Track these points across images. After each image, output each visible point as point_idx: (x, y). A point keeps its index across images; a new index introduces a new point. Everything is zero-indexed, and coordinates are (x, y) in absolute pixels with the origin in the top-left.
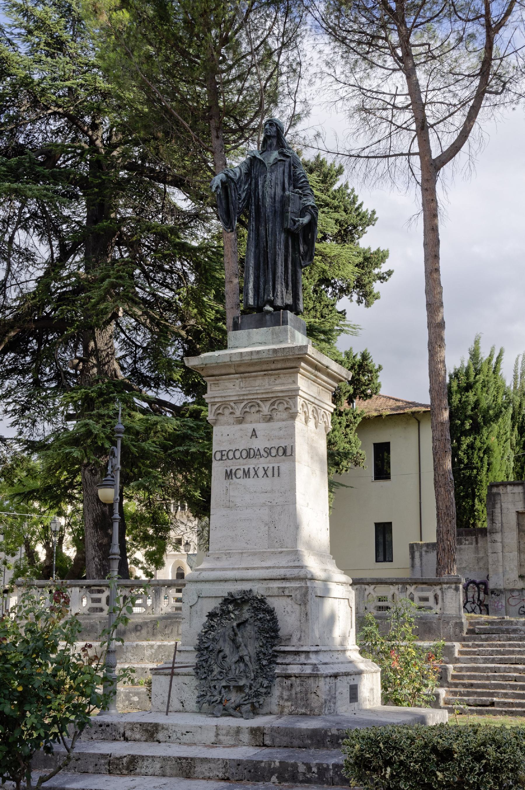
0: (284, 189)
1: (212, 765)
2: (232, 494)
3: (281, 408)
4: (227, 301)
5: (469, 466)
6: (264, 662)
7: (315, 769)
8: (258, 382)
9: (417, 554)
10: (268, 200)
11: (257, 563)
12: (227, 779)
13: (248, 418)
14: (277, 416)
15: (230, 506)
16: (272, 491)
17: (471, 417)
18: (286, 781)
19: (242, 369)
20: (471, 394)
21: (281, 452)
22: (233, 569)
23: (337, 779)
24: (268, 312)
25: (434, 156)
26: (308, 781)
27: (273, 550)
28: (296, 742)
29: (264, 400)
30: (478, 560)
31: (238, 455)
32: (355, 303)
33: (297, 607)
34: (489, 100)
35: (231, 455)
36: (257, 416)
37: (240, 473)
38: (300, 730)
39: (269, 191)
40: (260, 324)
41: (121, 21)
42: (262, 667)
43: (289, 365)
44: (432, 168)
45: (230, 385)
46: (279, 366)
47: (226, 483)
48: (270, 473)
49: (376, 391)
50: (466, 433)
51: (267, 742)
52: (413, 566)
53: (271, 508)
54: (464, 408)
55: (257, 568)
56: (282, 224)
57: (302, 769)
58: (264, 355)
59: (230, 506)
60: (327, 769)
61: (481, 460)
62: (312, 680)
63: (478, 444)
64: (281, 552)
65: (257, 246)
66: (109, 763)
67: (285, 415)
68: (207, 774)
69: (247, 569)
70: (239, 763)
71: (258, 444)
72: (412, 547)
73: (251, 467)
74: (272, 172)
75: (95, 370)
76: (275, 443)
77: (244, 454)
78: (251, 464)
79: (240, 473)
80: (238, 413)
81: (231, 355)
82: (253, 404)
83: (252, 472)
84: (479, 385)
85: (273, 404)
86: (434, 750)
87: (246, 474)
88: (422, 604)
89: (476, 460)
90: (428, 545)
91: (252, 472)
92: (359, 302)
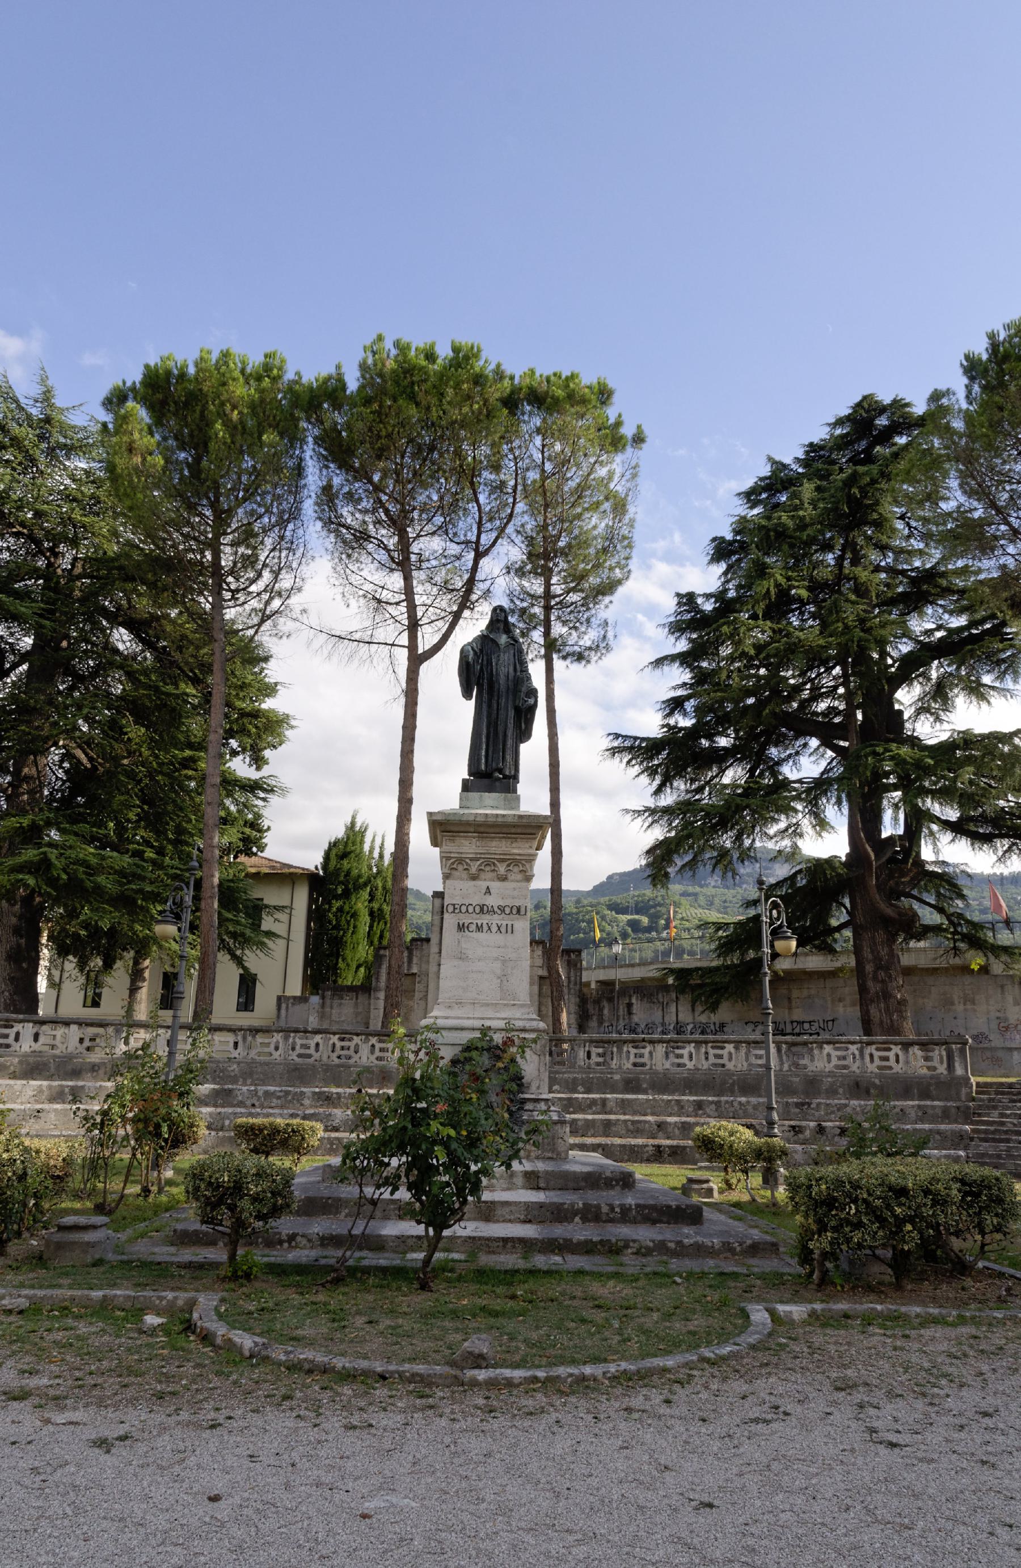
1: (513, 1208)
3: (516, 869)
4: (210, 750)
5: (337, 927)
7: (617, 1210)
8: (494, 843)
9: (284, 1006)
11: (490, 1014)
12: (530, 1221)
13: (483, 875)
14: (512, 876)
15: (462, 957)
16: (505, 947)
17: (342, 883)
18: (589, 1221)
19: (482, 829)
20: (345, 862)
23: (639, 1218)
25: (420, 651)
26: (611, 1221)
30: (357, 1014)
31: (471, 909)
32: (246, 766)
34: (466, 613)
37: (473, 927)
38: (575, 1172)
39: (503, 671)
40: (490, 790)
41: (155, 466)
42: (511, 1114)
44: (416, 660)
45: (466, 843)
46: (519, 831)
48: (503, 929)
49: (262, 848)
50: (337, 897)
51: (542, 1185)
52: (278, 1016)
53: (504, 962)
54: (338, 875)
56: (514, 701)
57: (605, 1209)
58: (510, 820)
59: (462, 957)
60: (630, 1209)
61: (348, 922)
62: (558, 1127)
63: (347, 908)
65: (489, 716)
66: (399, 1209)
67: (520, 877)
68: (508, 1217)
70: (541, 1205)
71: (492, 901)
75: (26, 797)
76: (509, 902)
77: (478, 909)
78: (484, 920)
79: (473, 927)
80: (474, 870)
82: (490, 863)
83: (485, 928)
84: (353, 855)
86: (891, 1188)
87: (479, 928)
88: (381, 1054)
89: (343, 922)
90: (295, 998)
91: (485, 928)
92: (250, 765)
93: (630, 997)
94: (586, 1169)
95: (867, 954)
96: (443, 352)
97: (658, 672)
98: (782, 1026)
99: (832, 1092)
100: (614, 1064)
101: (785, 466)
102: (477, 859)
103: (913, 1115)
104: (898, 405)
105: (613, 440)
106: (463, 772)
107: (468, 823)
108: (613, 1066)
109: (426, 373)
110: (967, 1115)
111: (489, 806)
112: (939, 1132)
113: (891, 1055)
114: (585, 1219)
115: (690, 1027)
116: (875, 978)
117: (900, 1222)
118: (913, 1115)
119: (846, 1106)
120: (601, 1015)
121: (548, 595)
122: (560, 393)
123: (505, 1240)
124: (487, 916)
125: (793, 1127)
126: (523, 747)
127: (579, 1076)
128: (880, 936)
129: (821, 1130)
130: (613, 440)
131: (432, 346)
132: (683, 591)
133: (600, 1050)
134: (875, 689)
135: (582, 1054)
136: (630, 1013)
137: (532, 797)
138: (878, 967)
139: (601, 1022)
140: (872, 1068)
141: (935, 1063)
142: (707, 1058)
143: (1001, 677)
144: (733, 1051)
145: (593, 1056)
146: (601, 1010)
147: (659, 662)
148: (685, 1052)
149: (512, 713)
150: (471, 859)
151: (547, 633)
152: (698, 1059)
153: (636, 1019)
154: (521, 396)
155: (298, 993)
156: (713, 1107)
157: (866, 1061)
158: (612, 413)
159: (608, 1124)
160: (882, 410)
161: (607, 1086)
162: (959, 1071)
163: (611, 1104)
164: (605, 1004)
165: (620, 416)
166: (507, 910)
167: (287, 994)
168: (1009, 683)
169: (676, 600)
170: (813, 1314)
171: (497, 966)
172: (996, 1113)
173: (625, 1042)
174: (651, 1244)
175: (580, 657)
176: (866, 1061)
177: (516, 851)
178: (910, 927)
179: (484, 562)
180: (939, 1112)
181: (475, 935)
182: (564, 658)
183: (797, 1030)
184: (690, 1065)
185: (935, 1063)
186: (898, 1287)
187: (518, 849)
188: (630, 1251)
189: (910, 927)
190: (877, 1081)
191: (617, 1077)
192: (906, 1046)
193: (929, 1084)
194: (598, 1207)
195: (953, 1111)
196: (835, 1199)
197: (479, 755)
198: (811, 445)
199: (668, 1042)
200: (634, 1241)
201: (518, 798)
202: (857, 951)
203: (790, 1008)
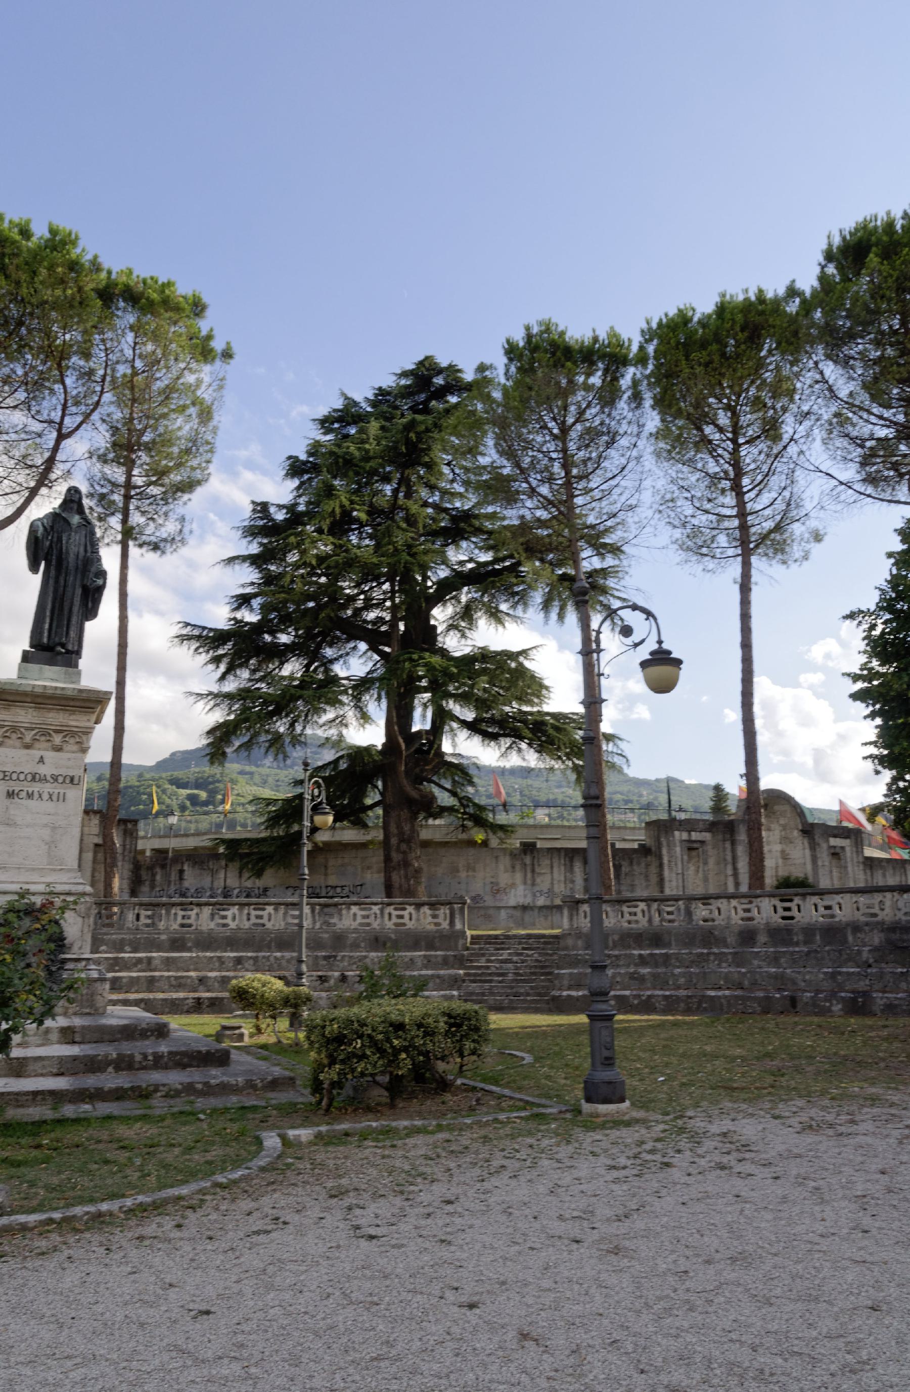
0: (86, 551)
1: (46, 1063)
2: (12, 812)
3: (72, 741)
6: (54, 969)
7: (150, 1058)
8: (51, 715)
10: (72, 555)
11: (35, 877)
12: (62, 1074)
13: (37, 745)
18: (122, 1070)
19: (39, 700)
21: (68, 781)
22: (12, 882)
23: (171, 1064)
24: (61, 653)
26: (144, 1068)
28: (106, 1037)
31: (22, 777)
33: (80, 920)
34: (44, 491)
35: (14, 776)
38: (111, 1026)
39: (73, 550)
42: (50, 973)
43: (87, 705)
45: (22, 712)
46: (78, 704)
47: (8, 802)
48: (55, 798)
51: (77, 1039)
53: (54, 828)
57: (138, 1058)
58: (69, 693)
60: (162, 1057)
62: (98, 984)
65: (56, 591)
67: (75, 748)
68: (40, 1071)
70: (75, 1058)
71: (43, 770)
73: (36, 790)
74: (76, 532)
76: (64, 772)
77: (29, 777)
78: (36, 788)
79: (23, 795)
80: (28, 738)
81: (34, 686)
82: (45, 733)
85: (65, 737)
87: (30, 796)
91: (36, 795)
93: (183, 864)
94: (125, 1022)
95: (393, 829)
96: (40, 231)
97: (228, 570)
98: (318, 891)
99: (355, 946)
100: (162, 925)
101: (356, 404)
102: (32, 729)
103: (419, 964)
104: (452, 370)
105: (203, 351)
107: (25, 694)
108: (161, 927)
109: (18, 248)
110: (460, 961)
112: (438, 976)
113: (405, 913)
114: (118, 1069)
115: (236, 892)
116: (398, 850)
117: (397, 1051)
118: (419, 963)
119: (366, 957)
120: (153, 880)
121: (128, 485)
122: (155, 296)
123: (35, 1093)
125: (320, 977)
126: (88, 625)
127: (127, 937)
128: (405, 814)
129: (344, 978)
130: (203, 351)
131: (28, 222)
132: (259, 500)
133: (149, 913)
134: (417, 607)
135: (131, 916)
136: (181, 879)
138: (402, 840)
139: (152, 887)
140: (389, 925)
141: (440, 920)
142: (249, 919)
143: (514, 607)
144: (272, 912)
145: (142, 918)
146: (154, 875)
147: (231, 560)
148: (229, 913)
149: (79, 591)
150: (27, 729)
151: (125, 521)
152: (241, 920)
153: (186, 884)
154: (117, 292)
156: (251, 962)
157: (384, 918)
158: (204, 326)
159: (151, 981)
160: (440, 371)
161: (153, 945)
162: (458, 926)
163: (156, 962)
164: (158, 870)
165: (212, 330)
166: (60, 779)
168: (519, 611)
169: (251, 507)
170: (319, 1136)
171: (46, 833)
172: (484, 959)
173: (174, 905)
174: (180, 1087)
175: (156, 547)
176: (384, 918)
178: (429, 808)
179: (65, 443)
180: (440, 959)
181: (24, 802)
182: (141, 546)
183: (330, 894)
184: (233, 925)
185: (440, 920)
186: (392, 1106)
187: (76, 721)
188: (159, 1094)
189: (429, 808)
190: (393, 936)
191: (163, 937)
192: (418, 906)
193: (434, 937)
194: (132, 1056)
195: (451, 959)
196: (345, 1036)
197: (42, 628)
198: (380, 389)
199: (213, 904)
200: (164, 1085)
201: (79, 673)
202: (386, 827)
203: (326, 875)
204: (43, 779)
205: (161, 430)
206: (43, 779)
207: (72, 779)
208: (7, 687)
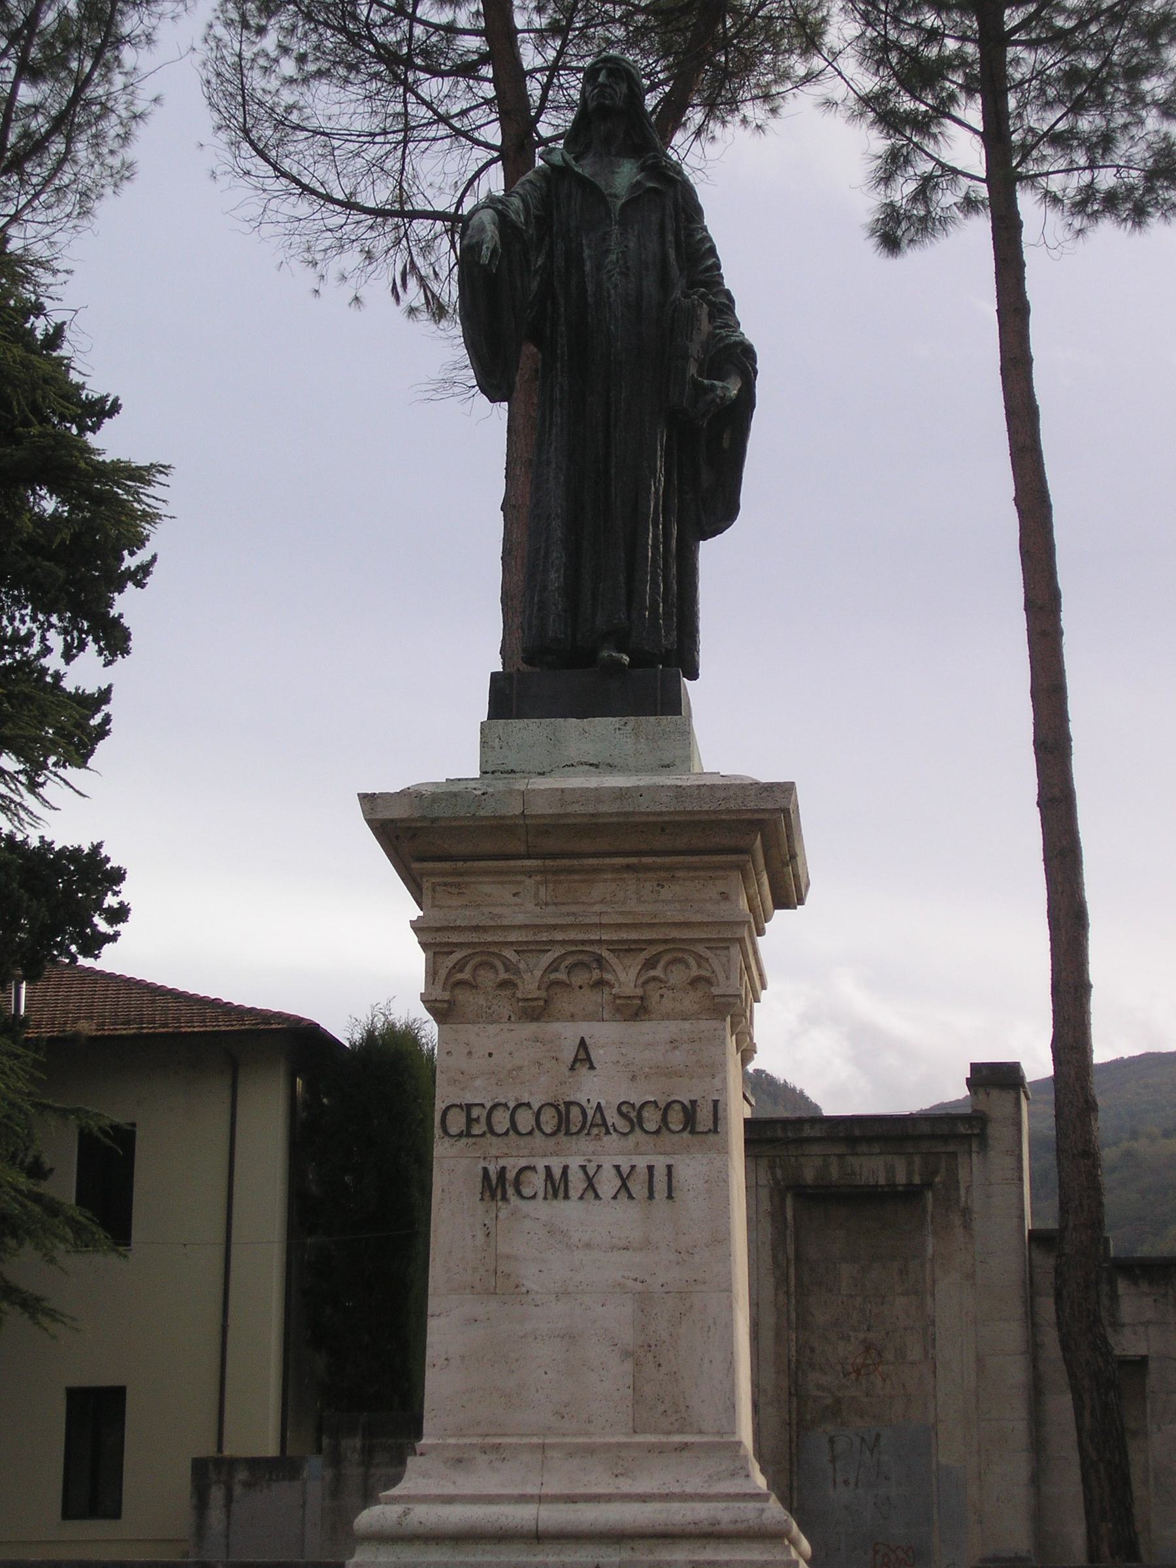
3: (678, 976)
8: (599, 890)
9: (217, 1495)
13: (563, 1003)
16: (646, 1244)
21: (676, 1119)
22: (523, 1499)
27: (652, 1438)
29: (627, 949)
31: (525, 1120)
35: (501, 1121)
36: (591, 999)
48: (638, 1187)
55: (609, 1498)
58: (644, 806)
64: (685, 1447)
67: (689, 1001)
69: (572, 1499)
71: (597, 1090)
72: (200, 1467)
73: (574, 1163)
77: (549, 1121)
78: (573, 1157)
79: (536, 1182)
80: (530, 985)
83: (577, 1182)
85: (650, 964)
87: (557, 1187)
90: (254, 1464)
91: (577, 1182)
106: (479, 646)
111: (588, 763)
124: (584, 1144)
137: (732, 724)
150: (522, 949)
155: (270, 1448)
166: (652, 1120)
167: (227, 1452)
177: (673, 913)
181: (542, 1210)
201: (685, 734)
204: (595, 1123)
205: (100, 127)
206: (595, 1123)
207: (690, 1114)
208: (439, 811)
